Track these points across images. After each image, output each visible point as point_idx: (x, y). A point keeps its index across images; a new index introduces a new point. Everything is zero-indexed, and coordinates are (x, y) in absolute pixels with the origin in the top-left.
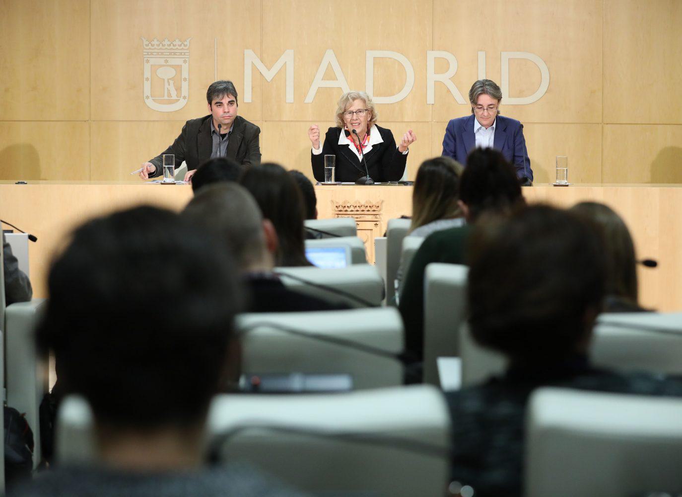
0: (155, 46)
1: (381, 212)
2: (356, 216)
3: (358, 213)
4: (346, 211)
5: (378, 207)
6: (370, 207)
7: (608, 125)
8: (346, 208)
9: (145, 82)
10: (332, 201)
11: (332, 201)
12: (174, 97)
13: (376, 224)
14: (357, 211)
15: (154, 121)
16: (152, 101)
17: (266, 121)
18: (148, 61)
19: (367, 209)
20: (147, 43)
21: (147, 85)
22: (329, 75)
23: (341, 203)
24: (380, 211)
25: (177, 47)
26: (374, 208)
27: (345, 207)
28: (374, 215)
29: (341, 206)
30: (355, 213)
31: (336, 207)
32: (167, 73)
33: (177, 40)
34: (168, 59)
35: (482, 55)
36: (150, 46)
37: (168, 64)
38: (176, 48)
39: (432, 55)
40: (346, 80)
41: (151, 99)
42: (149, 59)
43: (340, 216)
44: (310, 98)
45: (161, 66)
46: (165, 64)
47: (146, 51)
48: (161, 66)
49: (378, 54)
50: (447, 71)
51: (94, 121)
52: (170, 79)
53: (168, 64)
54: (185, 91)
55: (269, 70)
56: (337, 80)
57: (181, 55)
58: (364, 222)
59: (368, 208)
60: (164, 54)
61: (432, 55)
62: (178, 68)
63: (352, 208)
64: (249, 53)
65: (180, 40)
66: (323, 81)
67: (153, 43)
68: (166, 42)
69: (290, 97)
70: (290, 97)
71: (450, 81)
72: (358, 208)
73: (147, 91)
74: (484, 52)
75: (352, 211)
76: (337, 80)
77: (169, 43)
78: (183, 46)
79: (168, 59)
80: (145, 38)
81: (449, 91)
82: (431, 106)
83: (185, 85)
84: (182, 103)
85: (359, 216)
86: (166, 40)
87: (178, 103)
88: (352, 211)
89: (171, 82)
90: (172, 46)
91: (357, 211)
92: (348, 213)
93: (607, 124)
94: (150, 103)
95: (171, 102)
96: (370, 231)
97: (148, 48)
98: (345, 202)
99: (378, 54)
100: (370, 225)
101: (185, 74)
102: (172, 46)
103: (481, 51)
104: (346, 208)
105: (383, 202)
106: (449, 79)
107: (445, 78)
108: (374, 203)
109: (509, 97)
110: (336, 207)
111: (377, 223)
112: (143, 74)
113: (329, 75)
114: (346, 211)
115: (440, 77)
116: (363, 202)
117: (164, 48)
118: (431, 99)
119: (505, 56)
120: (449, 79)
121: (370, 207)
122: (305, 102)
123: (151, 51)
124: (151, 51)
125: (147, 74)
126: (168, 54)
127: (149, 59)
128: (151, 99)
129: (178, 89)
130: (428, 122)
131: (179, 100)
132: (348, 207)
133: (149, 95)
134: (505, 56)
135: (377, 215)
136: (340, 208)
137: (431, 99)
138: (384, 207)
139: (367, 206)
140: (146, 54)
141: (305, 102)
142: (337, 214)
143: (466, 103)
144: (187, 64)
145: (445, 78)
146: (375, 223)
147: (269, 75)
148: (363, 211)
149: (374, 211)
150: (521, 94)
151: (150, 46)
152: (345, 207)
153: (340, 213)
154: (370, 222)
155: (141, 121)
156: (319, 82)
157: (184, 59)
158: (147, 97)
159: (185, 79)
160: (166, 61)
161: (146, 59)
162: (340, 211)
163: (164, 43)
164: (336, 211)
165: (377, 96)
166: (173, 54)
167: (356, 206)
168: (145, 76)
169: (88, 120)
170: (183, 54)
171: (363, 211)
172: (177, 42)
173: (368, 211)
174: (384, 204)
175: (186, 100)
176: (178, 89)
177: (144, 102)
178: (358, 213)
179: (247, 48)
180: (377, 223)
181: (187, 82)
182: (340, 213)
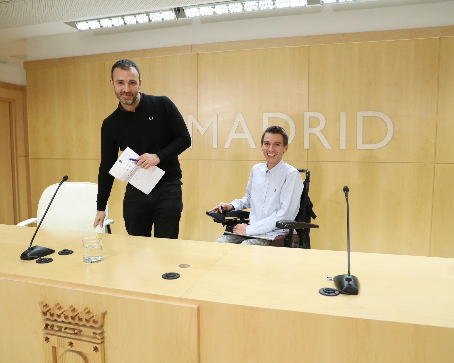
3: (71, 326)
6: (86, 320)
7: (438, 164)
13: (96, 349)
14: (70, 323)
17: (201, 160)
22: (239, 130)
24: (102, 326)
26: (91, 324)
30: (68, 326)
35: (343, 115)
44: (227, 146)
50: (316, 127)
55: (202, 128)
56: (244, 133)
58: (79, 342)
69: (215, 145)
70: (215, 145)
71: (320, 132)
72: (70, 320)
74: (345, 112)
75: (63, 322)
76: (244, 133)
81: (319, 140)
88: (63, 322)
91: (70, 323)
93: (438, 163)
105: (104, 314)
106: (320, 131)
107: (316, 131)
109: (363, 144)
113: (239, 130)
118: (306, 146)
119: (361, 115)
121: (86, 320)
122: (225, 147)
130: (305, 161)
137: (306, 146)
141: (225, 147)
143: (331, 148)
145: (316, 131)
146: (94, 345)
147: (202, 131)
150: (371, 142)
152: (53, 314)
154: (86, 343)
156: (233, 135)
162: (48, 319)
178: (71, 326)
182: (48, 322)
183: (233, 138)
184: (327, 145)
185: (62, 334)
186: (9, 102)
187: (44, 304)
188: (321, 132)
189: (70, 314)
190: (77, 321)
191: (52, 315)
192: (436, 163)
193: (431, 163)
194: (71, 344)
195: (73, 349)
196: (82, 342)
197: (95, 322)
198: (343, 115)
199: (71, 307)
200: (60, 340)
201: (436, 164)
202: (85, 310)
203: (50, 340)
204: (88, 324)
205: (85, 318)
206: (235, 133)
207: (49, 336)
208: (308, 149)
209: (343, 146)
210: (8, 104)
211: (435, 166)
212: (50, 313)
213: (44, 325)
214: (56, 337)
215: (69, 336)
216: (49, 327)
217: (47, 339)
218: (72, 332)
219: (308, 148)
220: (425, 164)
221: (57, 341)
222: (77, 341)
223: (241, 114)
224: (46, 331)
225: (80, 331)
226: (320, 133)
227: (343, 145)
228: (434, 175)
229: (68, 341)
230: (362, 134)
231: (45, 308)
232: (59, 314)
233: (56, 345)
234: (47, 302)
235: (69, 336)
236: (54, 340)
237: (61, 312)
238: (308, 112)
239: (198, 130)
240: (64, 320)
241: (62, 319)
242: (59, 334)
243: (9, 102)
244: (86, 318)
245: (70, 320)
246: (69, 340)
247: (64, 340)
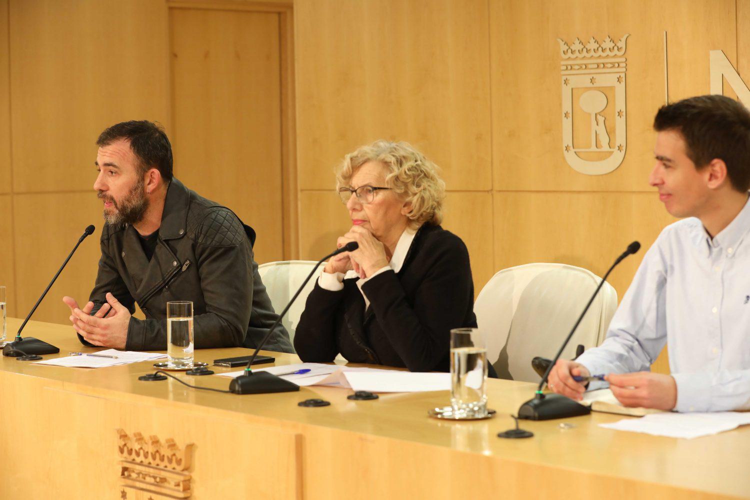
0: (577, 54)
1: (195, 475)
2: (148, 479)
9: (564, 119)
12: (606, 148)
15: (579, 192)
16: (574, 154)
18: (566, 82)
20: (565, 48)
21: (567, 124)
25: (608, 52)
32: (593, 103)
33: (608, 40)
34: (594, 76)
36: (569, 54)
37: (595, 85)
38: (604, 55)
41: (572, 151)
42: (568, 77)
45: (587, 89)
46: (591, 85)
47: (563, 63)
48: (587, 89)
51: (500, 191)
52: (599, 113)
53: (595, 85)
54: (620, 139)
57: (613, 67)
60: (590, 66)
62: (607, 92)
64: (716, 56)
65: (612, 41)
67: (573, 47)
68: (592, 45)
73: (567, 140)
77: (596, 46)
78: (616, 52)
79: (594, 76)
80: (563, 41)
83: (620, 123)
84: (618, 156)
86: (592, 41)
87: (611, 159)
88: (141, 464)
89: (601, 119)
90: (600, 52)
94: (571, 158)
95: (603, 156)
97: (566, 57)
101: (620, 105)
102: (600, 52)
105: (190, 447)
110: (121, 451)
112: (561, 105)
117: (588, 55)
123: (570, 62)
124: (570, 62)
125: (567, 107)
126: (597, 66)
127: (568, 77)
128: (572, 151)
129: (610, 132)
131: (613, 152)
133: (571, 145)
140: (565, 68)
144: (623, 83)
151: (569, 54)
155: (562, 192)
157: (618, 75)
158: (567, 149)
159: (619, 114)
160: (592, 80)
161: (564, 78)
163: (588, 46)
166: (602, 66)
168: (564, 111)
169: (492, 190)
170: (617, 65)
172: (608, 44)
174: (197, 454)
175: (623, 152)
176: (610, 132)
177: (564, 159)
178: (151, 471)
179: (715, 48)
181: (624, 118)
186: (279, 13)
187: (123, 434)
189: (150, 449)
190: (158, 461)
191: (130, 452)
197: (179, 462)
202: (167, 441)
207: (127, 490)
210: (275, 18)
212: (128, 448)
213: (121, 470)
216: (126, 473)
218: (152, 480)
224: (123, 482)
225: (164, 480)
231: (121, 440)
232: (137, 449)
237: (139, 447)
239: (738, 97)
241: (141, 458)
242: (138, 484)
243: (279, 13)
245: (150, 459)
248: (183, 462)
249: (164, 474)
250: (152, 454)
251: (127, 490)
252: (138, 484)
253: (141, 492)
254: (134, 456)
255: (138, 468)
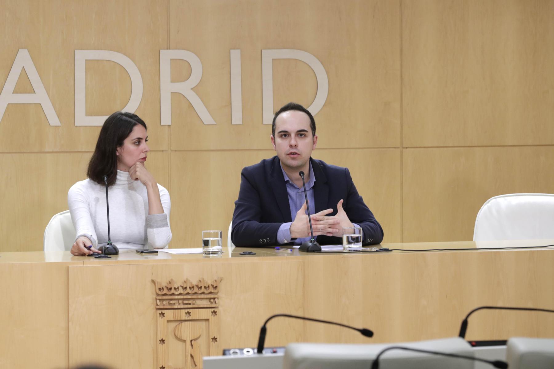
1: (219, 294)
2: (186, 302)
3: (189, 297)
4: (173, 294)
5: (216, 287)
6: (205, 287)
7: (408, 149)
8: (173, 291)
10: (153, 281)
11: (153, 281)
14: (188, 294)
19: (201, 292)
23: (164, 284)
24: (217, 293)
26: (211, 290)
27: (171, 289)
28: (210, 299)
29: (165, 289)
30: (185, 297)
31: (160, 289)
35: (236, 55)
39: (167, 56)
40: (49, 96)
43: (164, 303)
49: (93, 55)
56: (35, 93)
58: (197, 310)
59: (203, 290)
61: (167, 56)
63: (180, 290)
66: (14, 94)
72: (188, 290)
75: (180, 294)
81: (191, 106)
82: (167, 126)
85: (190, 302)
88: (180, 294)
91: (188, 294)
92: (176, 297)
93: (407, 148)
96: (204, 323)
98: (170, 283)
99: (93, 55)
100: (206, 314)
103: (234, 49)
104: (173, 291)
105: (221, 280)
106: (191, 89)
108: (210, 282)
110: (160, 289)
111: (216, 310)
114: (173, 294)
115: (179, 87)
116: (195, 283)
119: (269, 56)
120: (191, 89)
121: (205, 287)
130: (163, 151)
132: (175, 289)
134: (269, 56)
135: (214, 299)
136: (165, 291)
138: (222, 287)
139: (201, 287)
142: (160, 300)
143: (215, 123)
146: (212, 310)
148: (196, 293)
149: (211, 293)
152: (171, 289)
153: (164, 297)
154: (204, 309)
164: (158, 295)
165: (91, 115)
167: (186, 288)
171: (196, 293)
173: (203, 293)
178: (189, 297)
180: (216, 310)
183: (8, 104)
184: (207, 118)
185: (179, 307)
188: (195, 92)
192: (404, 148)
193: (395, 148)
194: (189, 313)
195: (190, 318)
196: (200, 310)
198: (236, 55)
199: (187, 279)
200: (176, 312)
201: (404, 150)
203: (165, 315)
204: (207, 291)
205: (204, 286)
206: (13, 93)
208: (169, 126)
209: (237, 119)
211: (402, 152)
214: (172, 311)
215: (186, 306)
217: (162, 314)
219: (170, 124)
220: (386, 149)
221: (173, 314)
222: (195, 310)
223: (26, 50)
226: (192, 93)
227: (237, 119)
228: (402, 170)
229: (185, 312)
230: (271, 93)
232: (177, 287)
233: (172, 319)
234: (159, 280)
235: (186, 306)
236: (169, 314)
238: (167, 49)
240: (182, 292)
244: (205, 286)
246: (186, 311)
247: (180, 312)
248: (218, 288)
249: (200, 296)
250: (190, 287)
251: (164, 311)
252: (176, 307)
253: (179, 310)
254: (173, 290)
255: (176, 297)
